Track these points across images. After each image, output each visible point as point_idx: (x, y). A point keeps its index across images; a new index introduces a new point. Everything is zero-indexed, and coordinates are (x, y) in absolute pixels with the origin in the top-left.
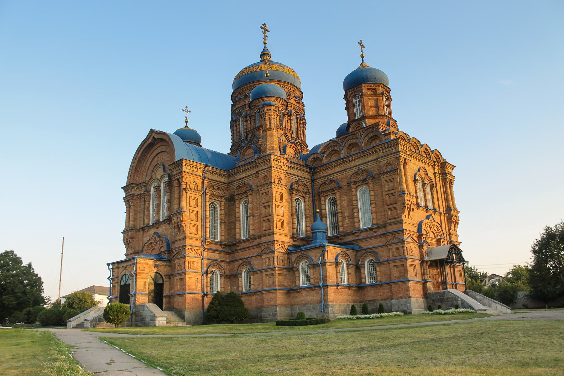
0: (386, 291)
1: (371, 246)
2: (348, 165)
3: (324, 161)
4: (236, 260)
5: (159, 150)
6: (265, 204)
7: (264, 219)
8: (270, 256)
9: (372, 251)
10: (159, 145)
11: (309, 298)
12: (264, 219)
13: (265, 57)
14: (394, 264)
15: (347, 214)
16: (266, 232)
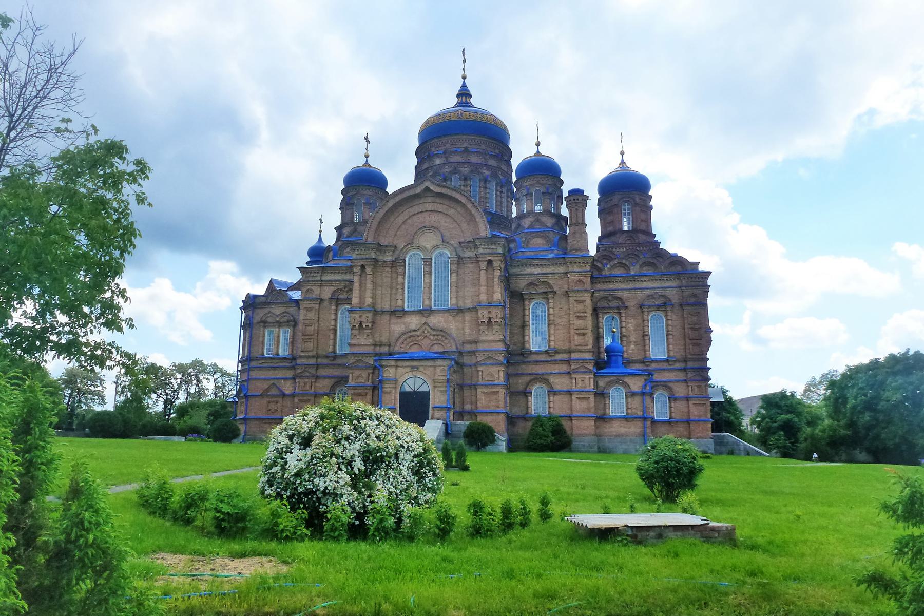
0: (681, 429)
1: (664, 379)
2: (638, 285)
3: (606, 272)
4: (522, 374)
5: (429, 207)
6: (578, 314)
7: (577, 331)
8: (584, 376)
9: (666, 385)
10: (430, 199)
11: (623, 430)
12: (577, 331)
13: (464, 97)
14: (694, 402)
15: (633, 339)
16: (579, 347)
